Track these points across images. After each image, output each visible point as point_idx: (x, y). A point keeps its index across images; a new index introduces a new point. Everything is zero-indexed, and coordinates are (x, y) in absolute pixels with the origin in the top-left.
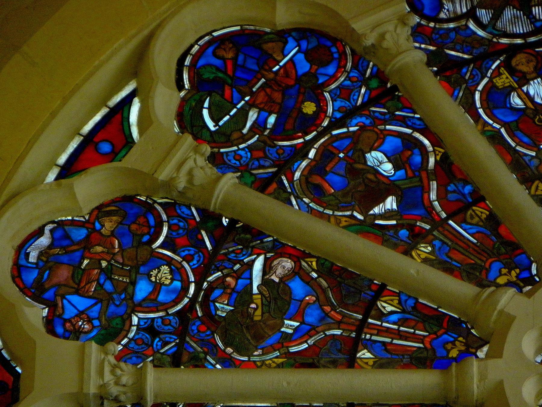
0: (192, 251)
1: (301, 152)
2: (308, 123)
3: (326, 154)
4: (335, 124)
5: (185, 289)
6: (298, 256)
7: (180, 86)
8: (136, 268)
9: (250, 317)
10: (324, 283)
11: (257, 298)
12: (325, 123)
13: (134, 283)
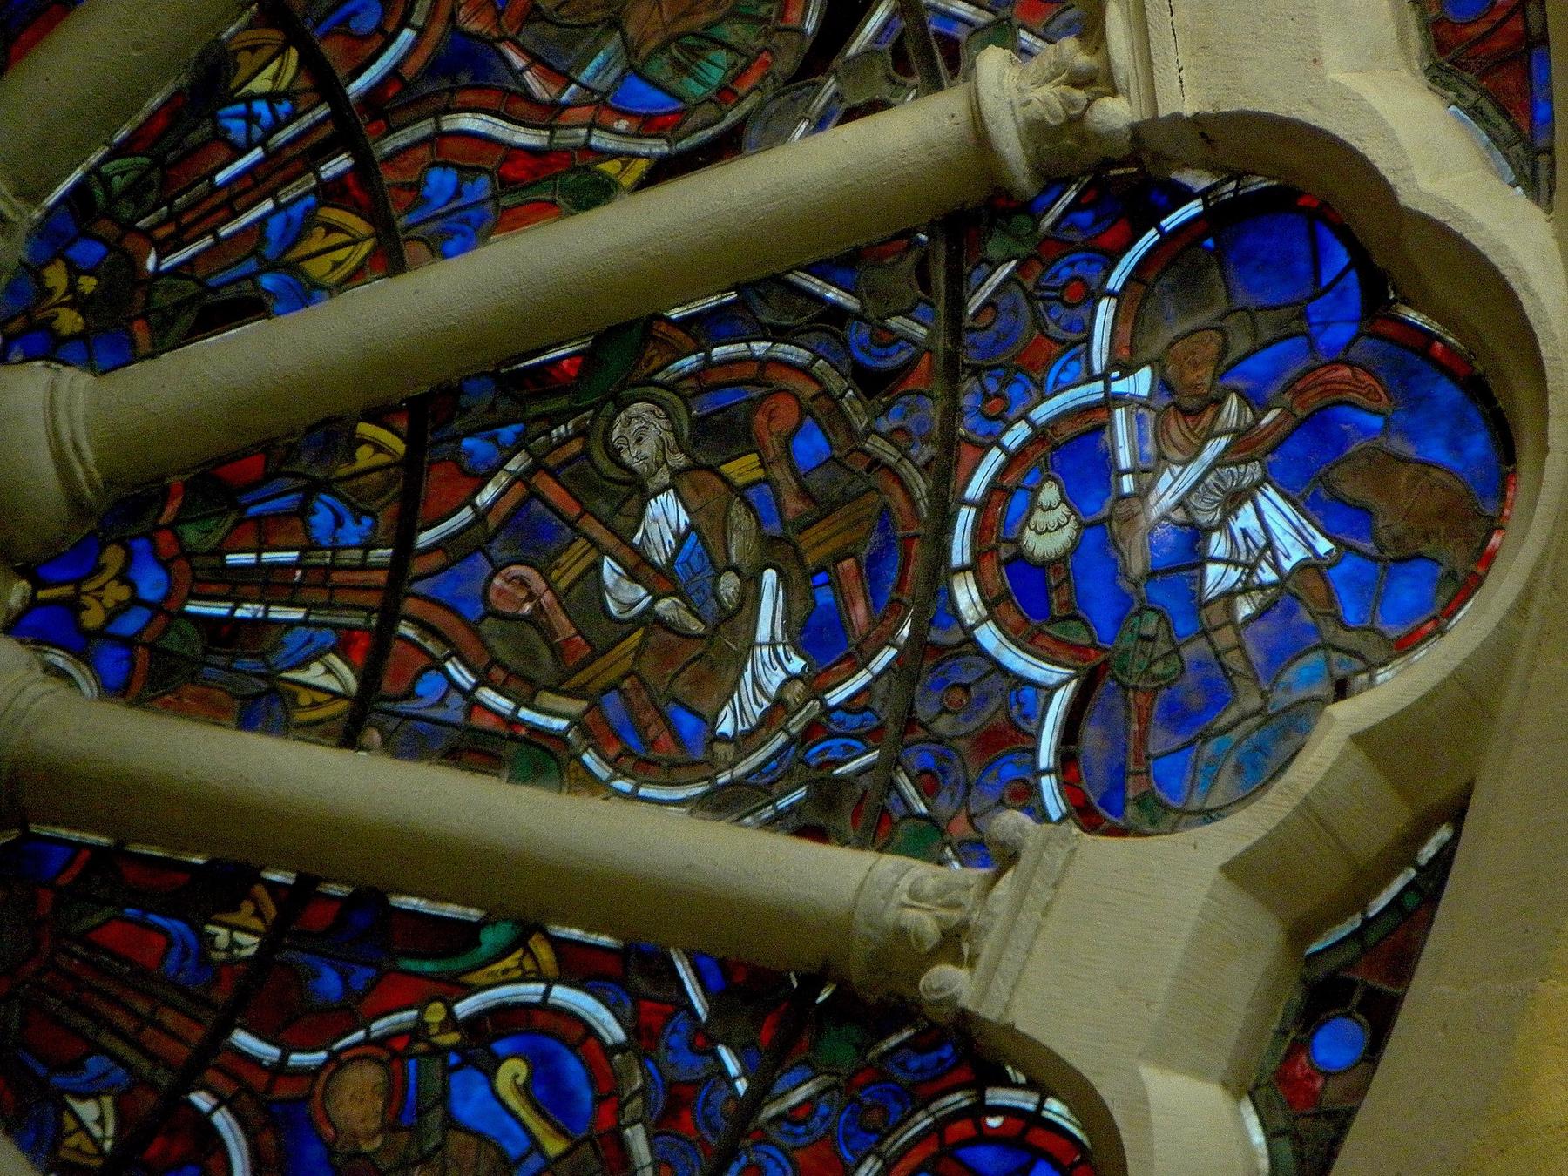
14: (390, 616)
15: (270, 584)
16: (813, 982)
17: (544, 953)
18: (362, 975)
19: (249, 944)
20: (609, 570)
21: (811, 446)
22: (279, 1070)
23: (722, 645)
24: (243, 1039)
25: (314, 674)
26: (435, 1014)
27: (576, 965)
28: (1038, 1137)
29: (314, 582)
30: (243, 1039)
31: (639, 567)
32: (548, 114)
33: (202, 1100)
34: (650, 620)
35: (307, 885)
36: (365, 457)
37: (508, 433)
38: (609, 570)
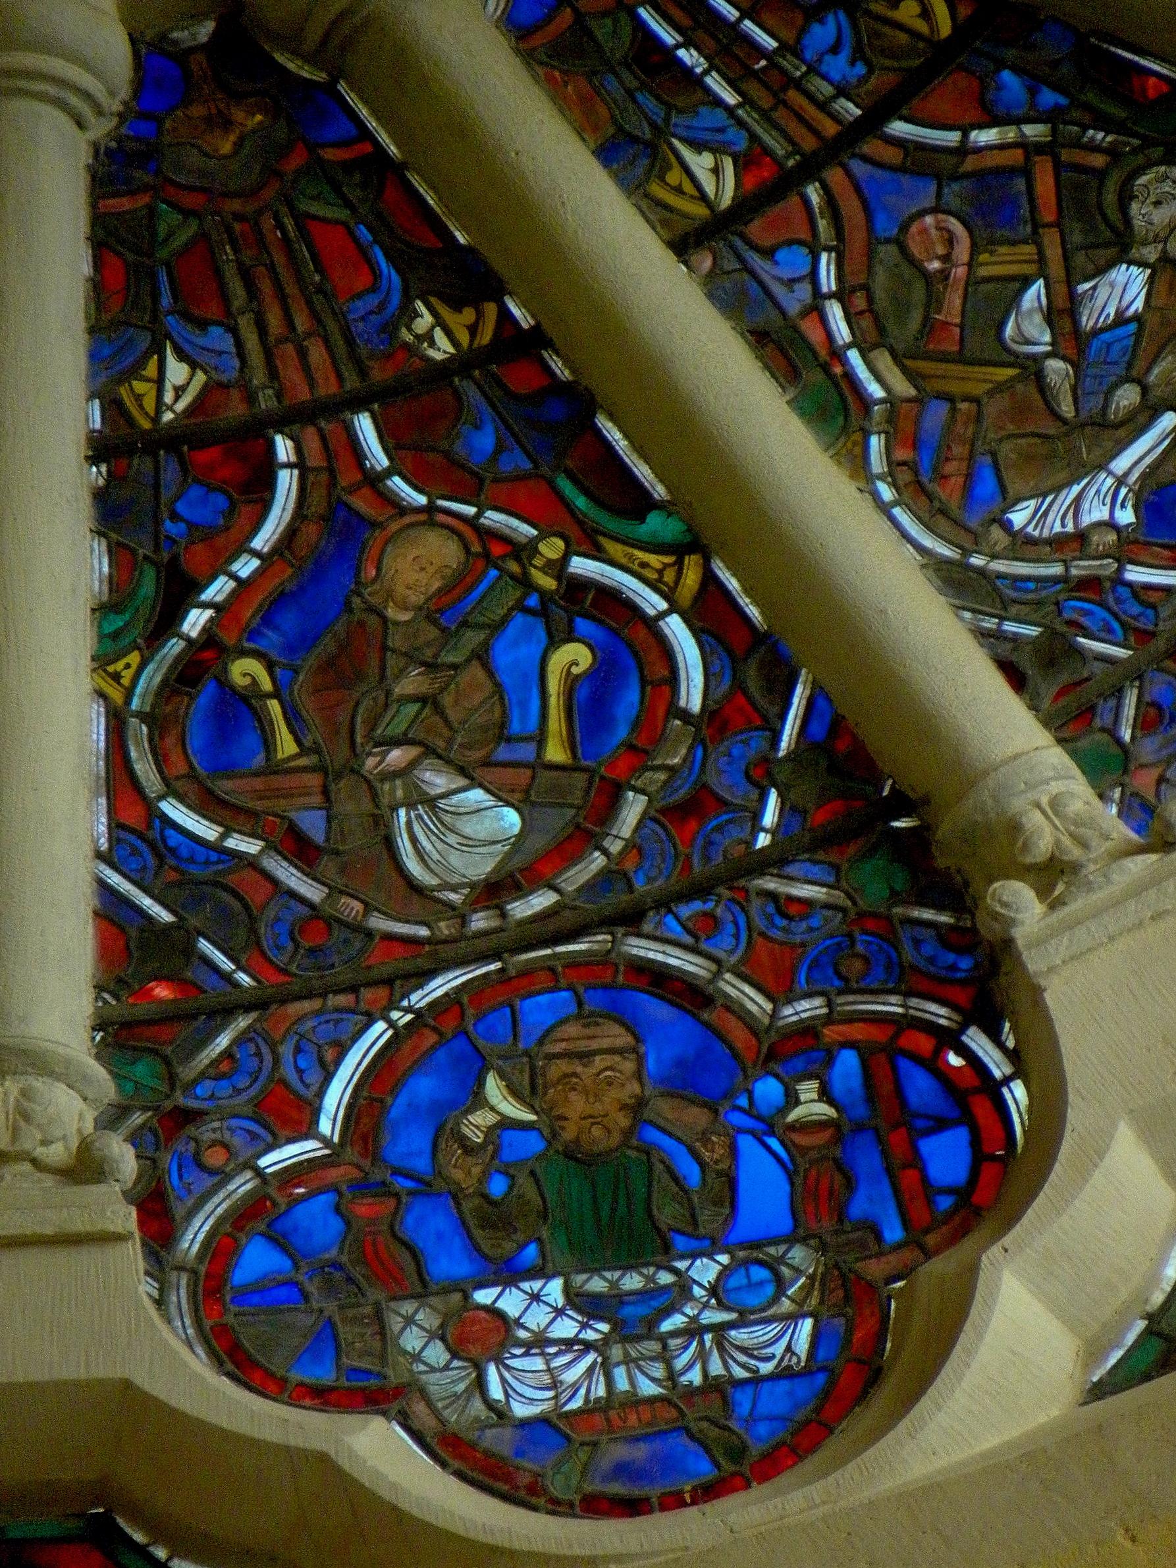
14: (810, 168)
17: (692, 577)
20: (1035, 294)
22: (374, 480)
25: (701, 163)
26: (552, 549)
27: (711, 613)
30: (365, 425)
31: (1062, 313)
33: (284, 448)
34: (1032, 369)
35: (537, 339)
38: (1035, 294)
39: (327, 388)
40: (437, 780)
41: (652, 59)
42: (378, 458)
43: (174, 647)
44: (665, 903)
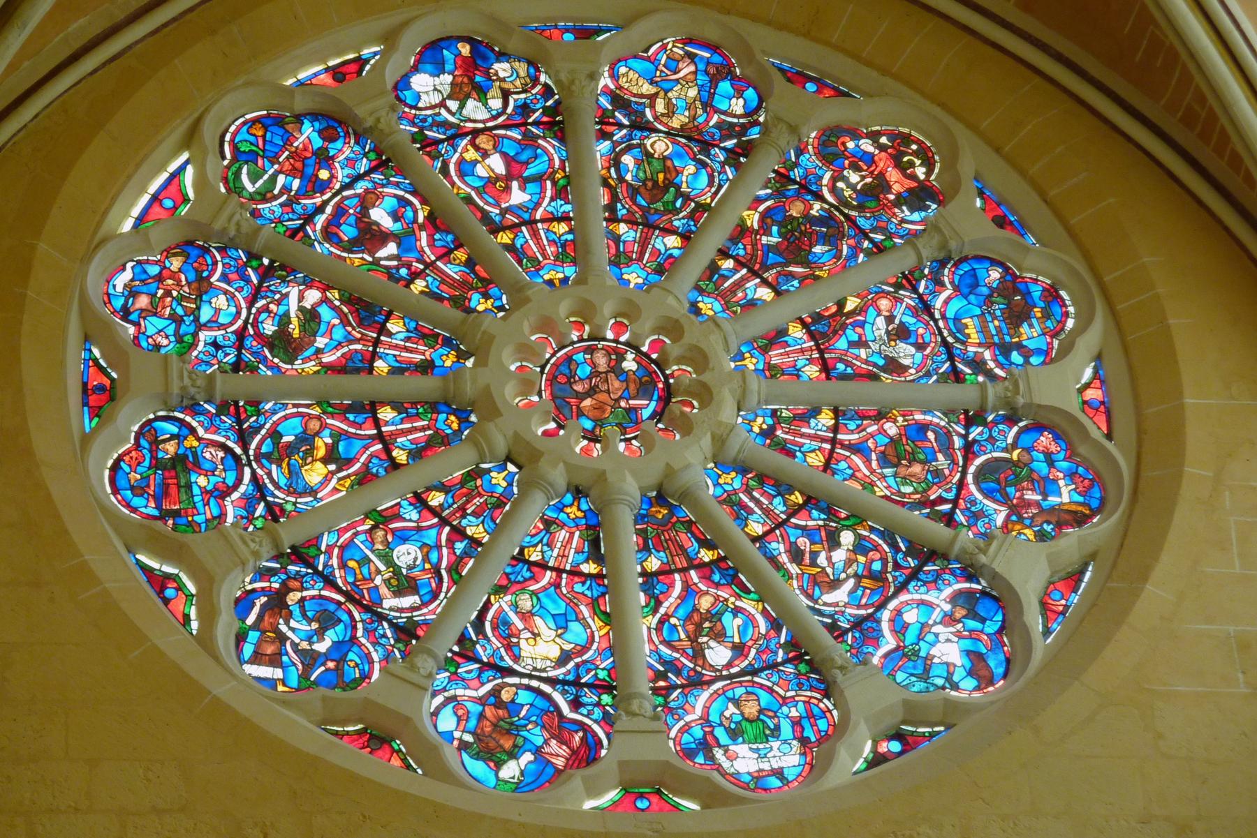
0: (242, 284)
1: (320, 209)
2: (323, 187)
3: (340, 211)
4: (345, 187)
5: (238, 313)
6: (325, 288)
7: (224, 158)
8: (200, 296)
9: (290, 335)
10: (345, 310)
11: (295, 321)
12: (337, 186)
13: (198, 308)
15: (758, 502)
16: (806, 653)
17: (761, 607)
18: (723, 581)
19: (706, 559)
21: (877, 566)
23: (835, 584)
24: (693, 573)
27: (765, 613)
28: (828, 715)
29: (767, 512)
31: (829, 559)
32: (873, 472)
34: (823, 569)
36: (793, 498)
37: (823, 516)
39: (686, 565)
40: (712, 643)
41: (743, 506)
42: (696, 580)
43: (658, 616)
44: (762, 670)
